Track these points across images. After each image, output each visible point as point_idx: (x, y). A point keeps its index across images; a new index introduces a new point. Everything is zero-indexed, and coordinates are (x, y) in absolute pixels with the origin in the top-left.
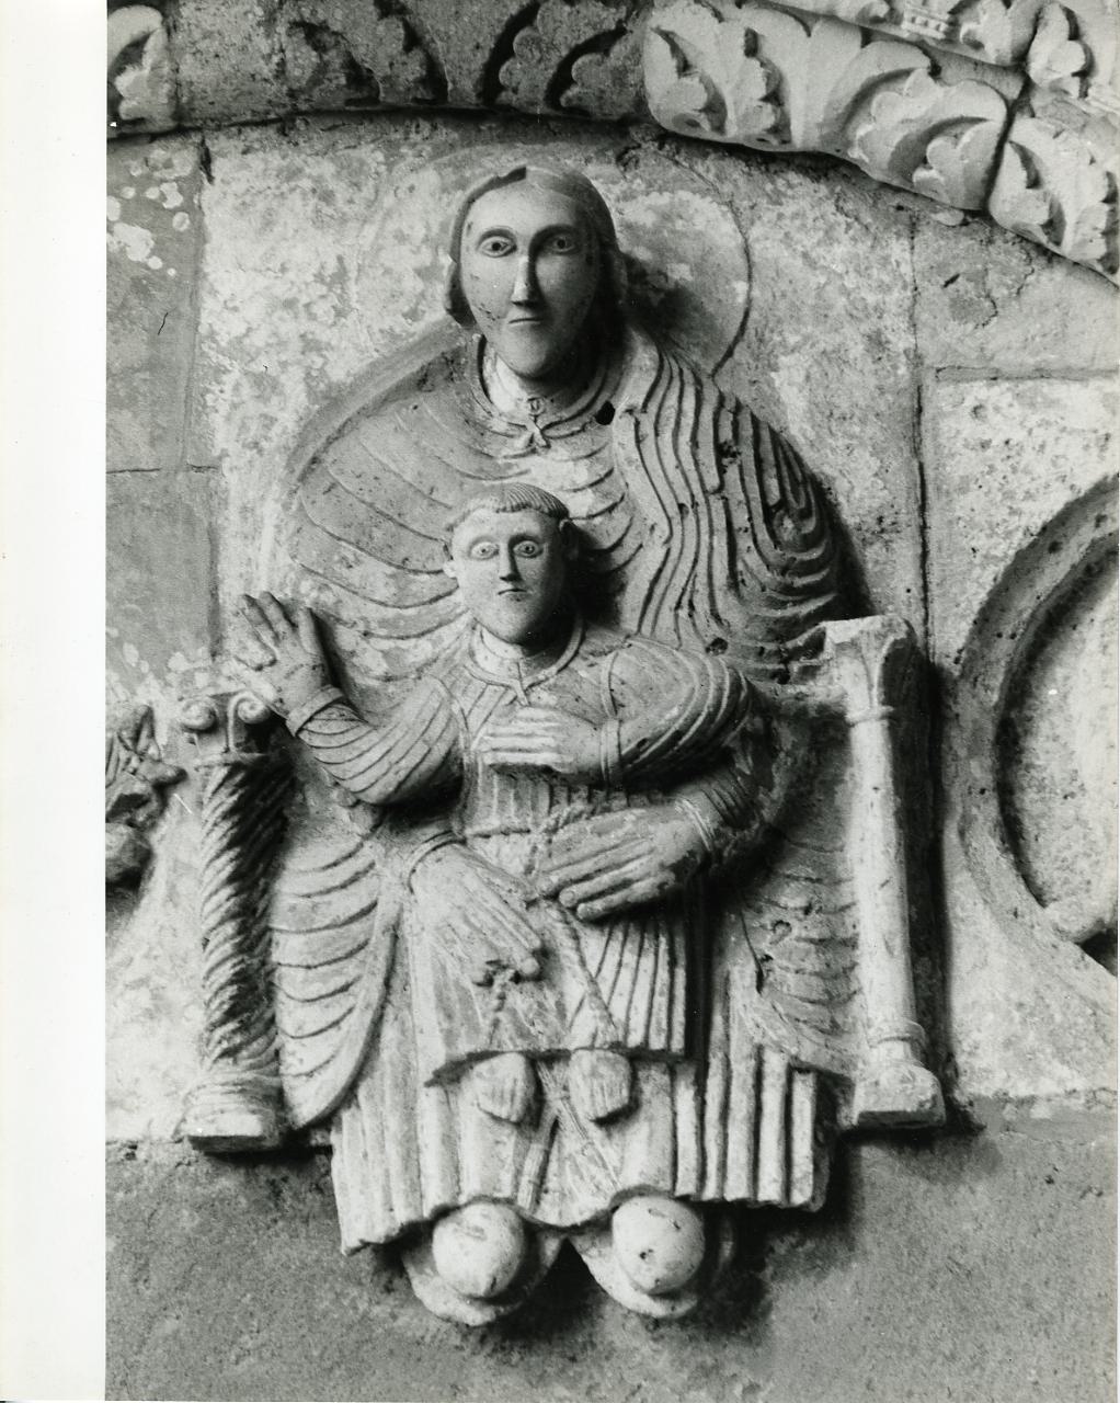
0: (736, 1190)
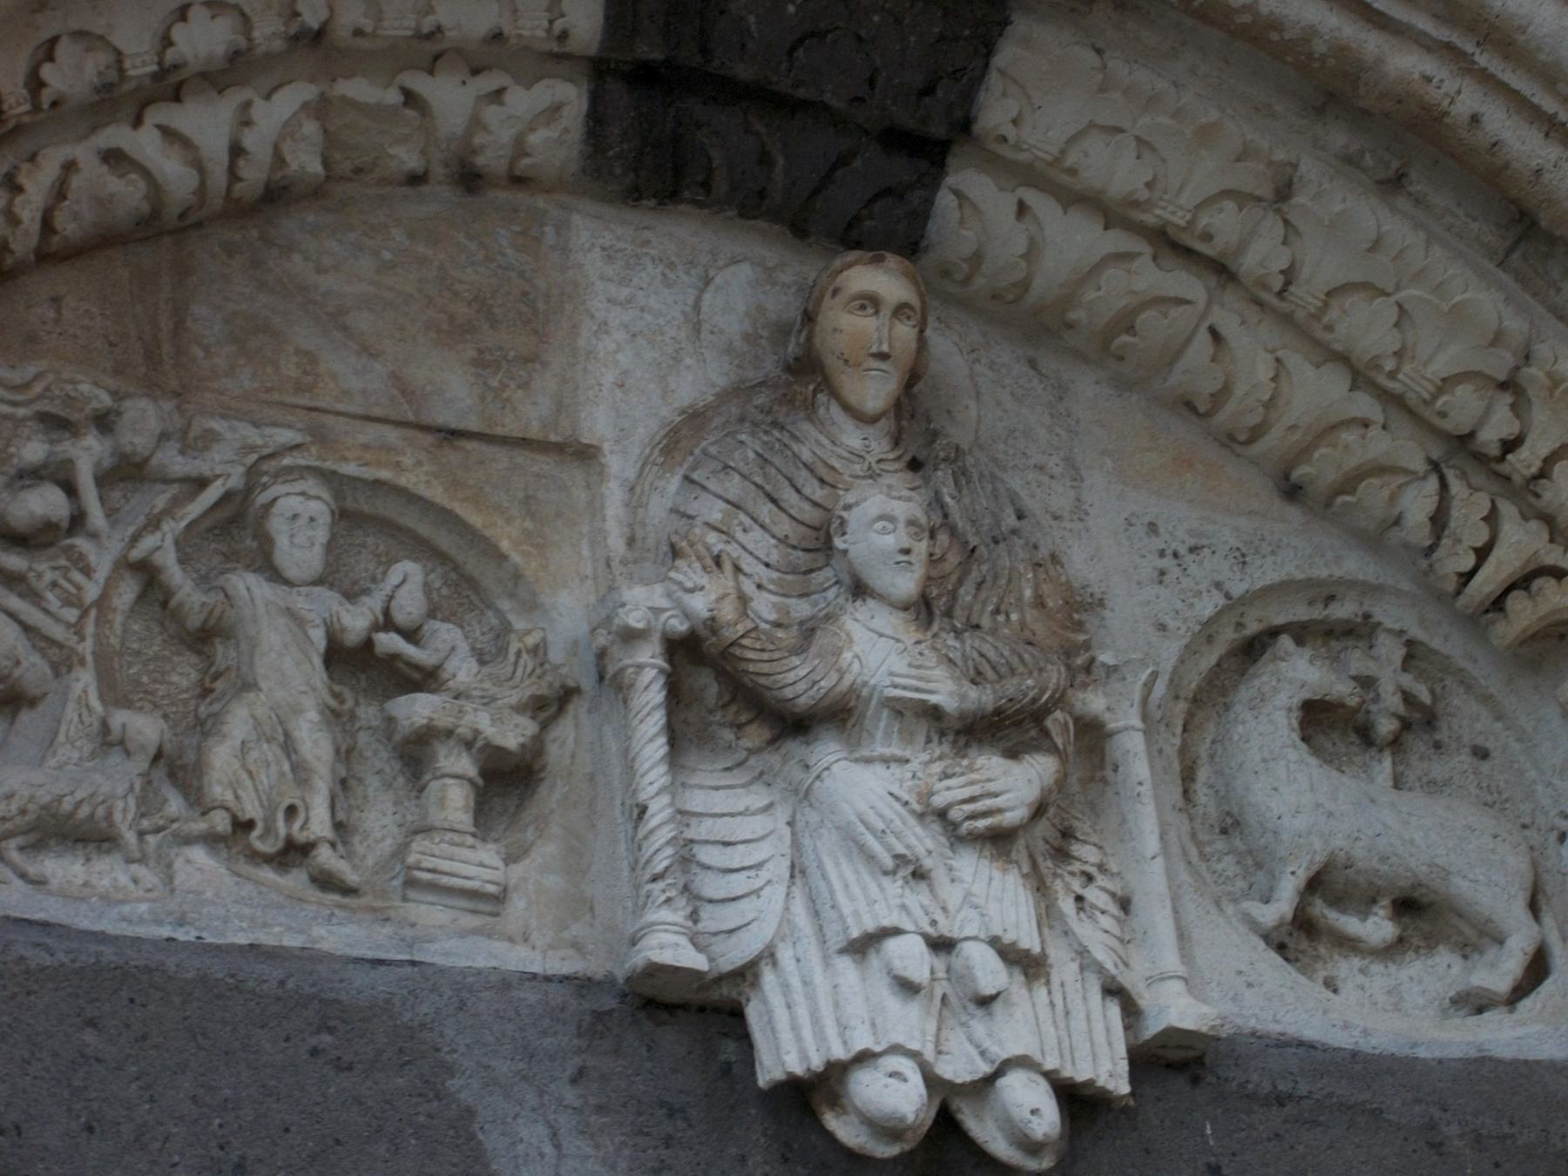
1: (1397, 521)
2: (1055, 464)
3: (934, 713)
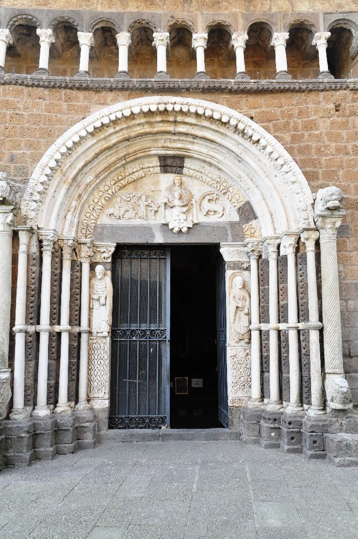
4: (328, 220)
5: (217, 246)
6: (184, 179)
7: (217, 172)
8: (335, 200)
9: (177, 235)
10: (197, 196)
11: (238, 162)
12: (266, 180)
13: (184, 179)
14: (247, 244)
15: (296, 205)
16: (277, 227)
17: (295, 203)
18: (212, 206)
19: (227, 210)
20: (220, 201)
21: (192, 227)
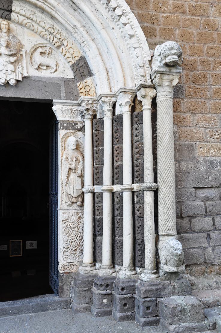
0: (17, 79)
1: (47, 38)
2: (22, 35)
3: (7, 54)
4: (166, 77)
5: (49, 104)
6: (12, 26)
7: (50, 21)
8: (175, 54)
9: (4, 88)
10: (28, 47)
11: (73, 10)
12: (103, 32)
13: (12, 26)
14: (82, 102)
15: (133, 62)
16: (113, 85)
17: (133, 60)
18: (45, 60)
19: (61, 65)
20: (53, 56)
21: (21, 79)
